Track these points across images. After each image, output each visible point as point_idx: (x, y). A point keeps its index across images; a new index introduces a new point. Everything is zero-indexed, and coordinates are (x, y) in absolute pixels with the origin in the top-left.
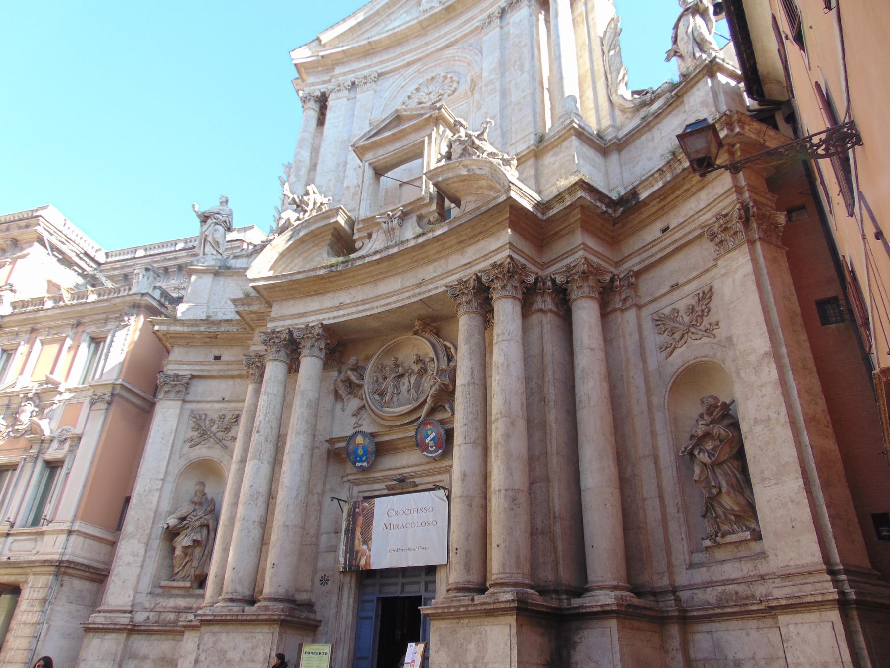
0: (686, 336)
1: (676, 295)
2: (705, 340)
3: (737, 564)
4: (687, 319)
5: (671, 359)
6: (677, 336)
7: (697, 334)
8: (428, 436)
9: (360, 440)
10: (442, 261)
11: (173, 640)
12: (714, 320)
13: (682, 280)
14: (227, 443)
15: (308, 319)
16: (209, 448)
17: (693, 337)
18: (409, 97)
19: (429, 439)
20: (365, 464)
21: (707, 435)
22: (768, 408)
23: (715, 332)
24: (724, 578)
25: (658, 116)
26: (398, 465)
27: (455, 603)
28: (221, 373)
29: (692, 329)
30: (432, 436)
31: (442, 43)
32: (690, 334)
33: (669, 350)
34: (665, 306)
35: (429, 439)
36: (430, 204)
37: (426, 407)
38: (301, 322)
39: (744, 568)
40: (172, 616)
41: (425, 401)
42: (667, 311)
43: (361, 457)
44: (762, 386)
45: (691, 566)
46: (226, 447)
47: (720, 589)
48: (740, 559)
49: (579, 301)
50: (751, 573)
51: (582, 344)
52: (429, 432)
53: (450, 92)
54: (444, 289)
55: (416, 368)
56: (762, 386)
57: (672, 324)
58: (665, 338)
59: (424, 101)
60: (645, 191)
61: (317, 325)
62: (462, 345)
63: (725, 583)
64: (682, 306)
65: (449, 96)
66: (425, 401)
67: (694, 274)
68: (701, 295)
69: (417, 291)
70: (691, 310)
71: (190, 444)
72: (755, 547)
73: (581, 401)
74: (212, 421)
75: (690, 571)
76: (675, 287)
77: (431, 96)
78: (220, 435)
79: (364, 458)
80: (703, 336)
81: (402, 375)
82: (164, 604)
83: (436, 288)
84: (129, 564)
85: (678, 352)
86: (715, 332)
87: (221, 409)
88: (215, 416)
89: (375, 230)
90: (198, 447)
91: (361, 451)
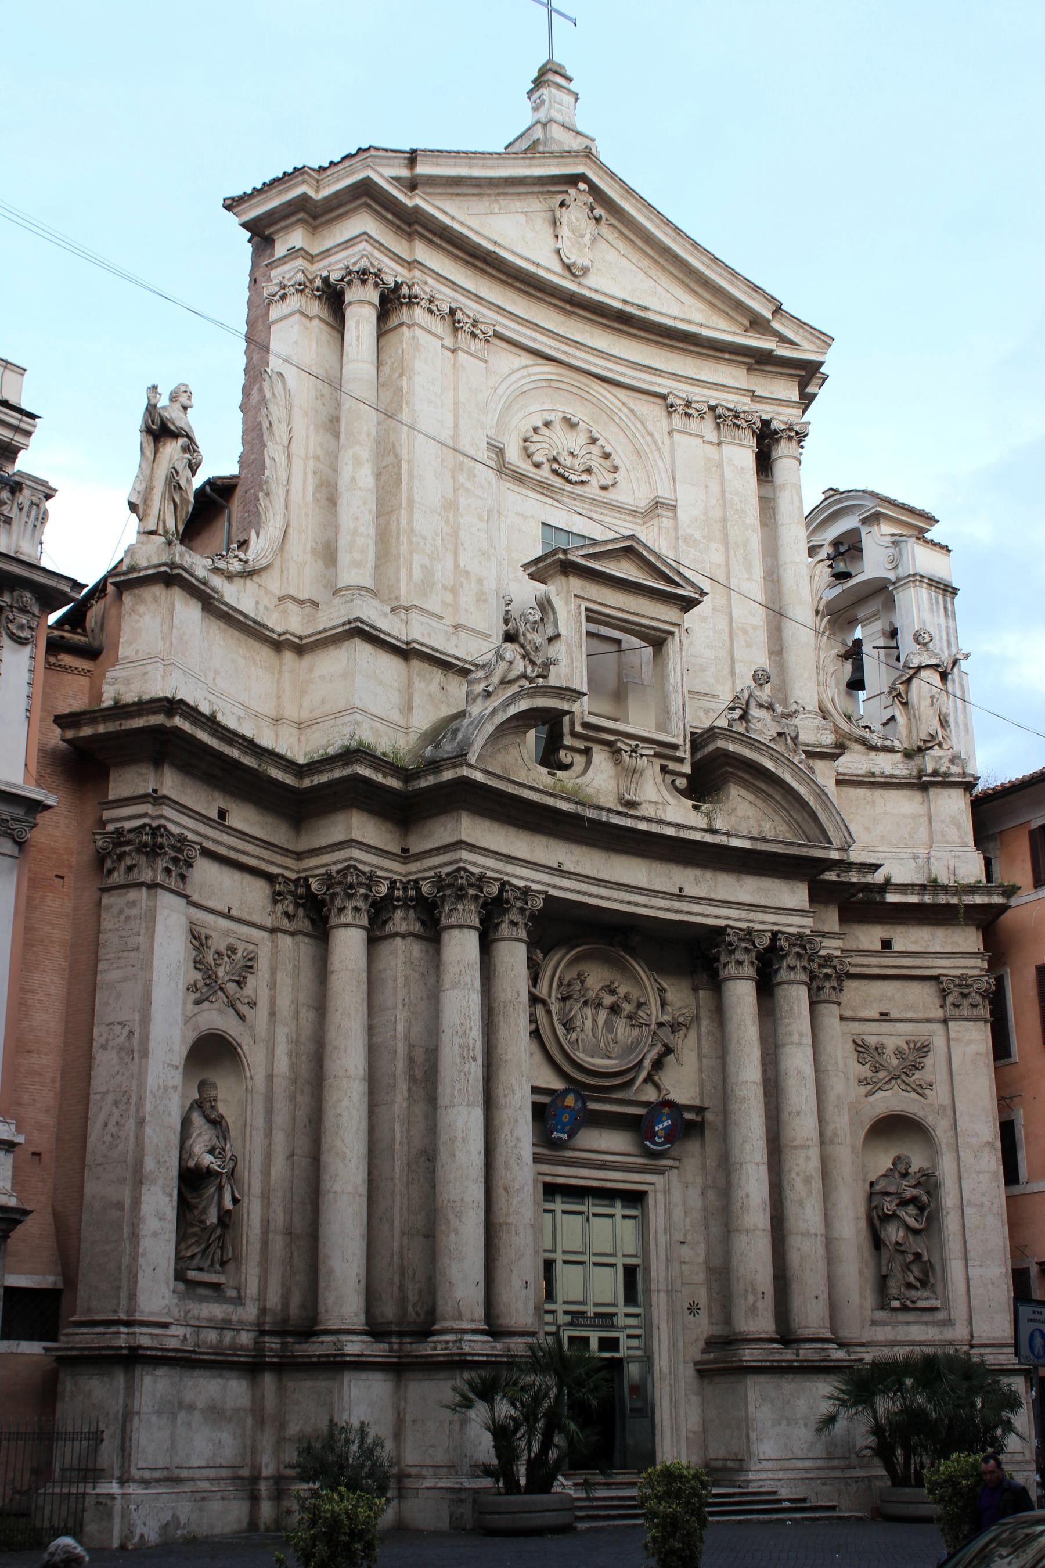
0: (893, 1081)
1: (885, 1027)
2: (914, 1095)
3: (923, 1328)
4: (895, 1062)
5: (871, 1099)
6: (881, 1074)
7: (907, 1084)
8: (662, 1122)
9: (570, 1100)
10: (708, 874)
11: (220, 1376)
12: (929, 1078)
13: (894, 1015)
14: (244, 1009)
15: (510, 868)
16: (221, 1011)
17: (903, 1086)
18: (535, 430)
19: (661, 1126)
20: (565, 1137)
21: (914, 1200)
22: (983, 1195)
23: (927, 1092)
24: (908, 1338)
25: (891, 784)
26: (595, 1146)
27: (777, 1357)
28: (233, 855)
29: (904, 1077)
30: (665, 1124)
31: (599, 365)
32: (899, 1081)
33: (869, 1087)
34: (873, 1034)
35: (661, 1126)
36: (681, 760)
37: (643, 1074)
38: (520, 877)
39: (930, 1331)
40: (212, 1336)
41: (639, 1064)
42: (872, 1041)
43: (564, 1125)
44: (979, 1172)
45: (874, 1323)
46: (242, 1017)
47: (908, 1349)
48: (926, 1323)
49: (832, 1005)
50: (937, 1338)
51: (836, 1063)
52: (664, 1118)
53: (604, 482)
54: (722, 923)
55: (608, 1000)
56: (979, 1172)
57: (877, 1058)
58: (865, 1071)
59: (562, 460)
60: (895, 893)
61: (539, 892)
62: (749, 1023)
63: (913, 1343)
64: (891, 1044)
65: (604, 488)
66: (639, 1064)
67: (909, 1015)
68: (919, 1045)
69: (677, 905)
70: (899, 1053)
71: (193, 997)
72: (941, 1316)
73: (836, 1135)
74: (219, 954)
75: (873, 1328)
76: (884, 1017)
77: (576, 462)
78: (231, 987)
79: (567, 1128)
80: (914, 1090)
81: (585, 1003)
82: (196, 1312)
83: (703, 915)
84: (155, 1234)
85: (880, 1094)
86: (927, 1092)
87: (227, 933)
88: (222, 948)
89: (596, 748)
90: (206, 1003)
91: (566, 1118)
